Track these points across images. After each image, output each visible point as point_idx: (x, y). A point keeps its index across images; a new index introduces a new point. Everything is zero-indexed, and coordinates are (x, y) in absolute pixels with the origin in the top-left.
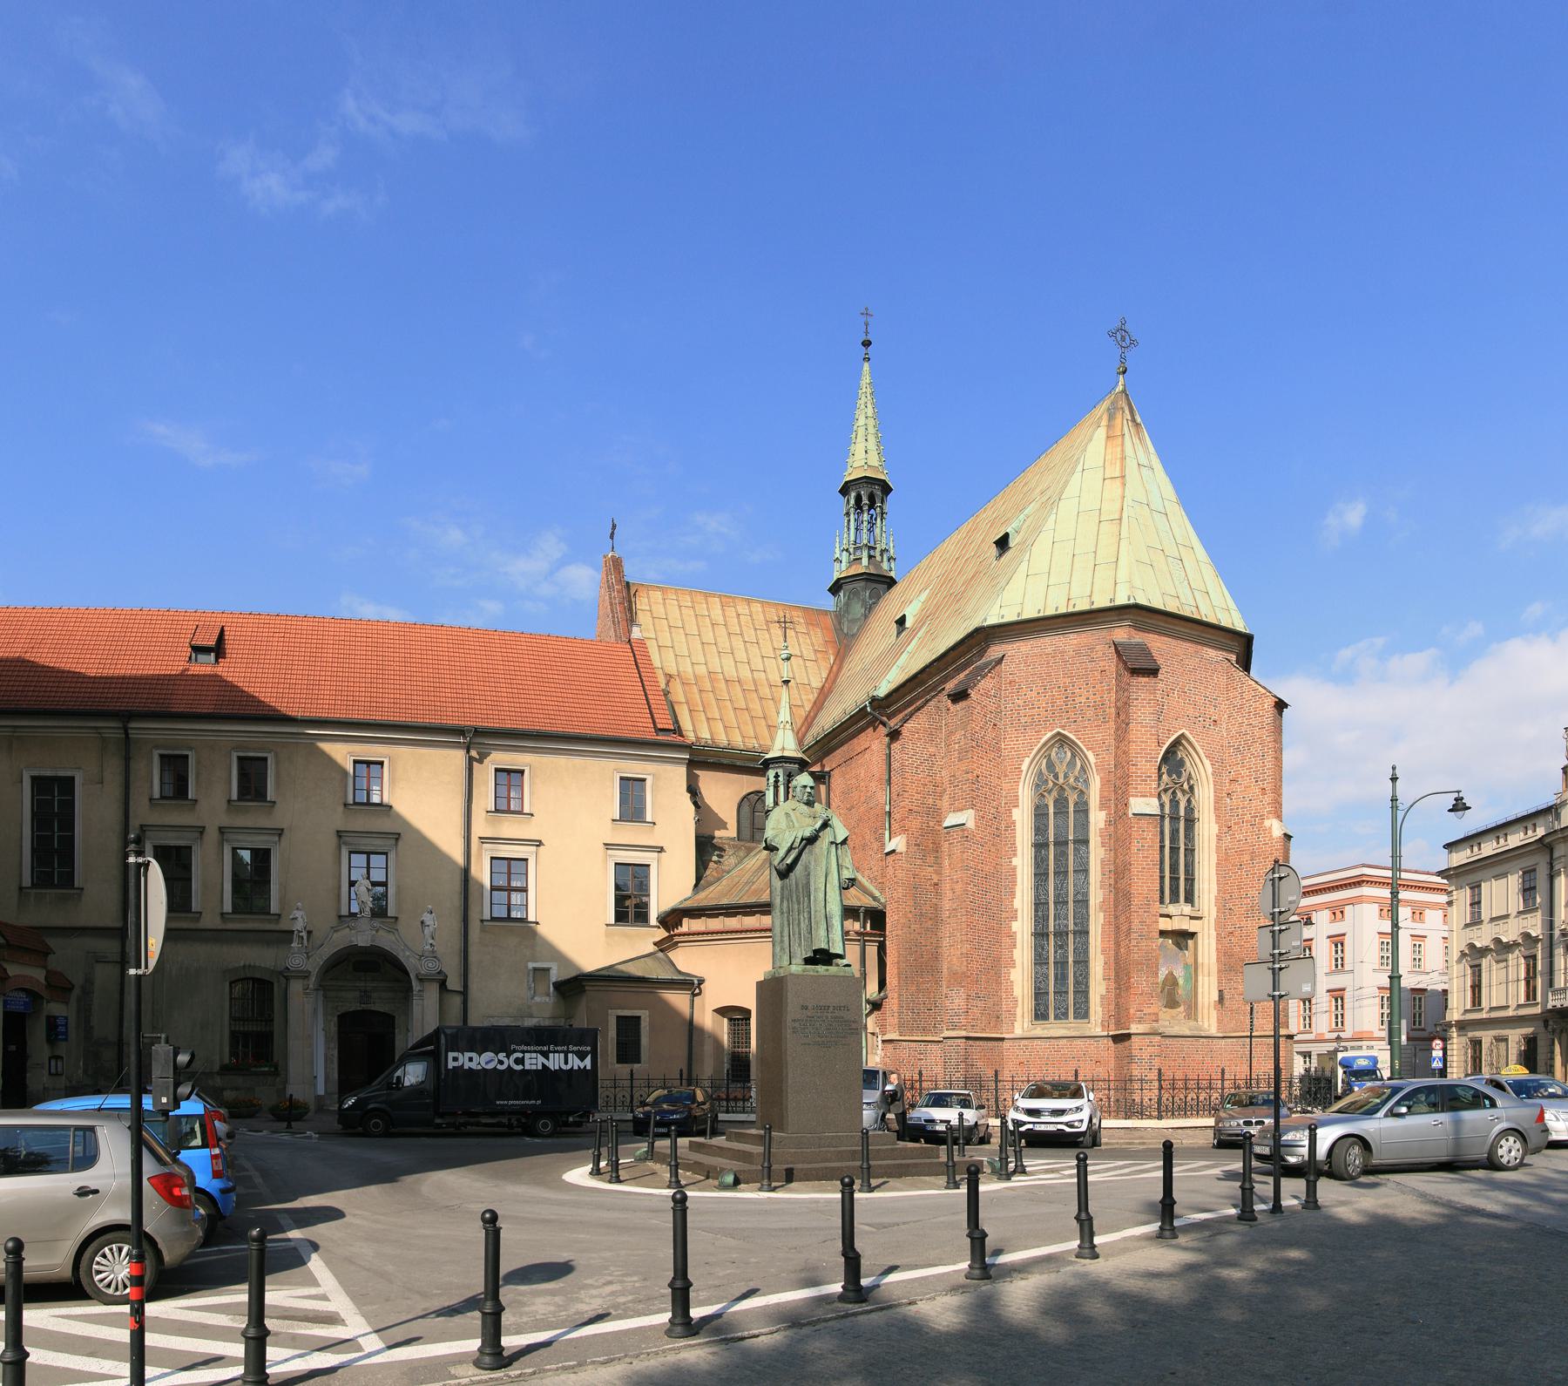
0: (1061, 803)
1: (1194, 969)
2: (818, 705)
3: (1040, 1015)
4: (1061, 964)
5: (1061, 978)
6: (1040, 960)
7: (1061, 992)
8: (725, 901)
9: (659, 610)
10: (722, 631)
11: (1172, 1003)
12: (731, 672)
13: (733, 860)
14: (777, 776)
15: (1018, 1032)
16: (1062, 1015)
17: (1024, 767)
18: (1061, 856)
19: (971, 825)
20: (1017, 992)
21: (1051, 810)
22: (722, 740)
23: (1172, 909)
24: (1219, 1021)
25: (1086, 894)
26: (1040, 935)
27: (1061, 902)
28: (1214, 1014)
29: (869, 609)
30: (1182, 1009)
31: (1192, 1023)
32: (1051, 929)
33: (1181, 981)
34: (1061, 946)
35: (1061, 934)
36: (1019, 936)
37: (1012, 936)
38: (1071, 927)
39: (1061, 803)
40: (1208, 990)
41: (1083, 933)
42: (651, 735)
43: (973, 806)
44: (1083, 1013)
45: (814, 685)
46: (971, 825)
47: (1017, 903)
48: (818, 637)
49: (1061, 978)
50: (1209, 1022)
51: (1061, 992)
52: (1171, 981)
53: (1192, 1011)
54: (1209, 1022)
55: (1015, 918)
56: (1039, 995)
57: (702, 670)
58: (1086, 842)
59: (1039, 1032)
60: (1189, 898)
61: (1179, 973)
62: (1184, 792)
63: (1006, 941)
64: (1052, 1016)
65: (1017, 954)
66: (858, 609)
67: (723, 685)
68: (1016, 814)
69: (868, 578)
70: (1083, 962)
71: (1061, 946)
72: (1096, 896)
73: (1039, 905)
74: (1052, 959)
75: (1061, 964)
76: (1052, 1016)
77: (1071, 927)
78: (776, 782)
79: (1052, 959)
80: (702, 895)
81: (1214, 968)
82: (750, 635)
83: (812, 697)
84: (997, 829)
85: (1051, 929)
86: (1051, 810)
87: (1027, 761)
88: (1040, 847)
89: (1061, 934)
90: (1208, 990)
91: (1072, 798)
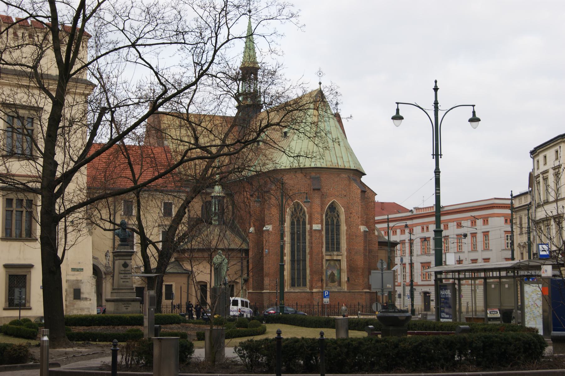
0: (298, 221)
1: (340, 271)
3: (293, 285)
4: (299, 270)
6: (293, 268)
7: (299, 278)
11: (333, 281)
16: (299, 285)
19: (271, 230)
23: (331, 253)
24: (348, 287)
26: (293, 261)
27: (298, 251)
28: (346, 285)
30: (336, 283)
31: (339, 287)
33: (336, 275)
35: (299, 261)
39: (298, 221)
40: (344, 278)
41: (304, 260)
44: (305, 285)
46: (271, 230)
52: (333, 275)
53: (340, 284)
54: (345, 288)
56: (293, 279)
59: (292, 290)
60: (338, 249)
61: (336, 272)
62: (335, 217)
70: (305, 269)
72: (308, 251)
75: (299, 270)
81: (346, 270)
89: (299, 261)
90: (344, 278)
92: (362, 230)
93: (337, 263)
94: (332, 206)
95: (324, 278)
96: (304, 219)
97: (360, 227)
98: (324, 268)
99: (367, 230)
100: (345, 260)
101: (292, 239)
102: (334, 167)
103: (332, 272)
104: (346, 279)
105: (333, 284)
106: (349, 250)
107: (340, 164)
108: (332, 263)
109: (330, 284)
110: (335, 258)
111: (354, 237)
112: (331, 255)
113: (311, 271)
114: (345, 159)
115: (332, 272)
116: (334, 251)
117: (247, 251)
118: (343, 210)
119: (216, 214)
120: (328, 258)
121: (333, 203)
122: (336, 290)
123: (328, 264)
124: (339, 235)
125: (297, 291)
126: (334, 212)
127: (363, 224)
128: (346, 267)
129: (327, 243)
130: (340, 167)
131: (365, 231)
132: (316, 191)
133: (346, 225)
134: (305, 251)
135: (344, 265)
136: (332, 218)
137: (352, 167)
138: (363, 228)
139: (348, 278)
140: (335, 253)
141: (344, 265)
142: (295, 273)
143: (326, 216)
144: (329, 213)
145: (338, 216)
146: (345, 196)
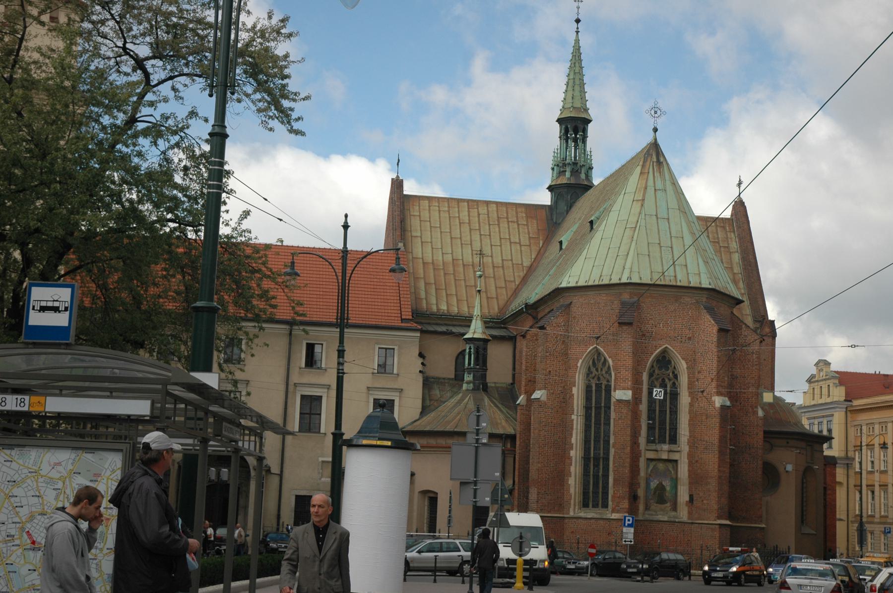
0: (598, 386)
1: (675, 482)
2: (525, 280)
4: (596, 477)
5: (596, 484)
7: (596, 493)
8: (428, 429)
9: (425, 215)
10: (466, 228)
11: (661, 500)
12: (468, 258)
13: (449, 394)
14: (470, 348)
15: (572, 514)
16: (595, 506)
17: (579, 365)
18: (598, 414)
19: (544, 398)
20: (572, 491)
21: (594, 389)
22: (455, 310)
23: (658, 447)
24: (690, 513)
25: (609, 437)
26: (586, 459)
27: (597, 441)
29: (570, 207)
30: (668, 504)
31: (673, 513)
32: (592, 455)
33: (668, 488)
34: (596, 465)
36: (574, 459)
37: (570, 458)
38: (602, 455)
40: (683, 495)
41: (606, 459)
42: (398, 323)
43: (545, 388)
44: (605, 506)
45: (525, 264)
47: (573, 440)
48: (533, 226)
49: (596, 484)
50: (683, 514)
51: (596, 493)
52: (661, 488)
53: (675, 508)
54: (683, 514)
55: (572, 448)
56: (585, 494)
57: (449, 258)
58: (610, 408)
59: (582, 515)
60: (674, 440)
61: (667, 484)
62: (670, 380)
63: (567, 461)
64: (591, 505)
65: (572, 469)
66: (562, 206)
67: (461, 269)
68: (575, 390)
69: (568, 186)
70: (606, 476)
71: (596, 465)
73: (587, 441)
74: (592, 473)
75: (596, 477)
76: (591, 505)
77: (602, 455)
78: (470, 352)
79: (592, 473)
80: (427, 419)
82: (485, 229)
83: (522, 274)
84: (564, 401)
85: (592, 455)
86: (594, 389)
87: (581, 361)
88: (588, 408)
89: (596, 459)
90: (683, 495)
91: (604, 382)
92: (718, 405)
93: (670, 466)
94: (664, 357)
95: (641, 492)
96: (608, 381)
97: (713, 398)
98: (642, 474)
99: (728, 403)
100: (686, 461)
101: (587, 417)
102: (667, 283)
103: (661, 484)
104: (687, 498)
105: (663, 506)
106: (692, 443)
107: (679, 277)
108: (661, 466)
109: (654, 506)
110: (665, 456)
111: (704, 417)
112: (657, 451)
113: (615, 480)
114: (692, 268)
115: (661, 484)
116: (664, 442)
117: (513, 438)
118: (685, 366)
119: (470, 370)
120: (651, 455)
121: (665, 351)
122: (666, 519)
123: (651, 467)
124: (676, 412)
125: (590, 515)
126: (667, 369)
127: (719, 394)
128: (687, 475)
129: (650, 428)
130: (679, 284)
131: (723, 407)
132: (625, 327)
133: (691, 394)
134: (607, 442)
135: (683, 470)
136: (663, 380)
137: (705, 284)
138: (718, 401)
139: (691, 496)
140: (666, 447)
141: (683, 470)
142: (589, 482)
143: (651, 375)
144: (657, 372)
145: (676, 377)
146: (690, 338)
